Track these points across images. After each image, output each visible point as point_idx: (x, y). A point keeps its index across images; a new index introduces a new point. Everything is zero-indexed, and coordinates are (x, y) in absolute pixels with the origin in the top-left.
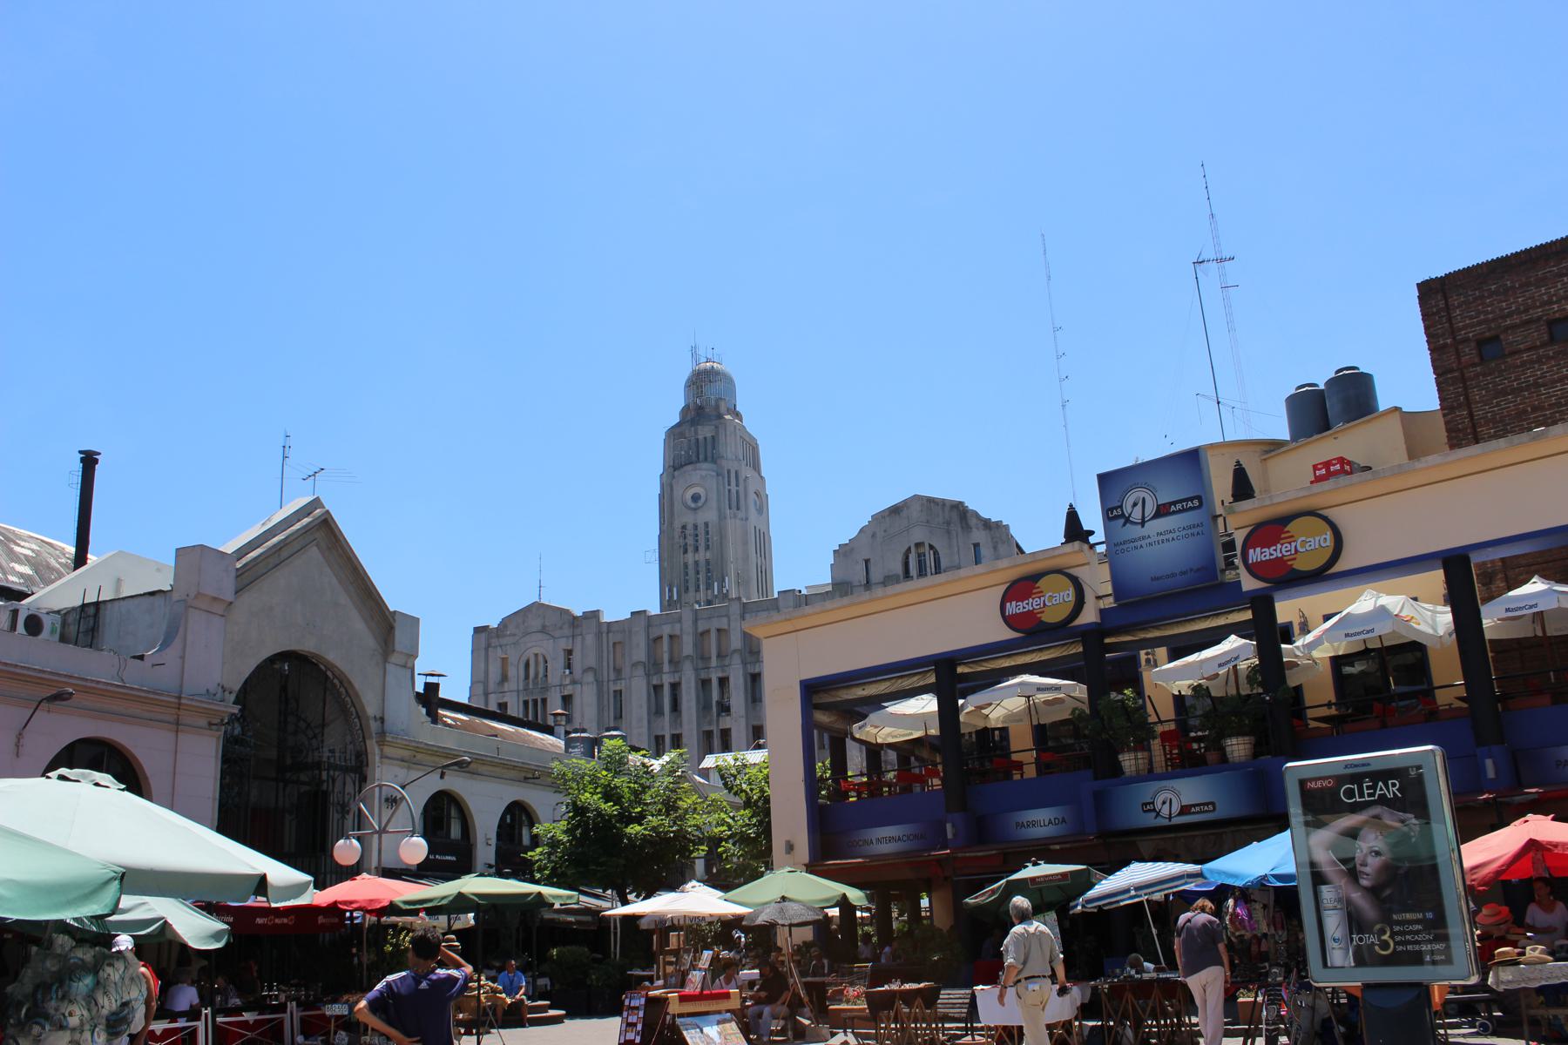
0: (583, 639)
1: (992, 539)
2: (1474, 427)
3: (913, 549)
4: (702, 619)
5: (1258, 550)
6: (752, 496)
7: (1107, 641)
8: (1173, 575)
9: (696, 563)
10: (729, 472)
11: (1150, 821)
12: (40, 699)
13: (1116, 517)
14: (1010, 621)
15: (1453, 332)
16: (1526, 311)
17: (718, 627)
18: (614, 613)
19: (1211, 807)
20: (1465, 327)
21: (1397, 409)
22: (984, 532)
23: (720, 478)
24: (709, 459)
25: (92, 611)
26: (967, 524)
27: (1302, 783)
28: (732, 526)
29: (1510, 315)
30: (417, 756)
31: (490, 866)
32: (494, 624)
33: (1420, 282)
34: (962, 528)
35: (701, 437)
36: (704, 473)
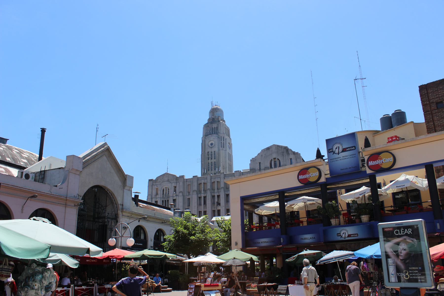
0: (179, 183)
1: (296, 157)
2: (435, 127)
4: (213, 178)
5: (371, 162)
6: (228, 144)
7: (328, 187)
8: (347, 169)
9: (212, 162)
10: (221, 137)
11: (339, 238)
12: (28, 197)
13: (331, 152)
14: (300, 181)
15: (429, 100)
17: (218, 181)
18: (188, 176)
19: (357, 235)
21: (412, 122)
23: (219, 139)
24: (216, 133)
25: (43, 173)
26: (288, 152)
27: (383, 229)
28: (222, 153)
30: (132, 215)
31: (152, 247)
32: (154, 179)
33: (419, 86)
34: (287, 154)
35: (213, 127)
36: (214, 137)
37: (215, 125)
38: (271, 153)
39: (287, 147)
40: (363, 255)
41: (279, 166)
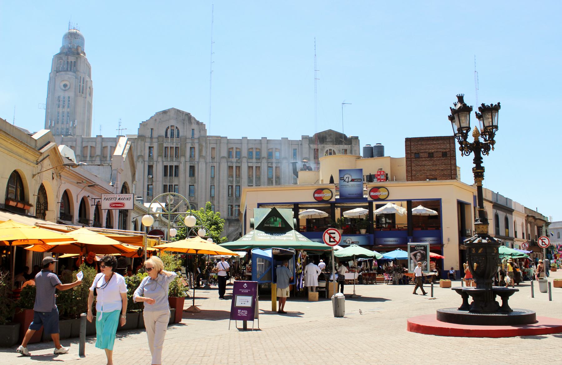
1: (199, 128)
2: (411, 171)
3: (170, 127)
4: (84, 141)
5: (373, 193)
6: (88, 89)
7: (336, 205)
8: (353, 194)
9: (63, 112)
10: (80, 77)
13: (342, 180)
14: (315, 198)
15: (411, 150)
16: (425, 150)
17: (91, 145)
20: (413, 150)
21: (390, 157)
22: (196, 125)
23: (77, 79)
24: (72, 71)
26: (191, 121)
29: (422, 150)
34: (189, 123)
35: (69, 61)
36: (70, 76)
37: (73, 58)
38: (169, 118)
39: (189, 114)
40: (390, 257)
41: (176, 136)
